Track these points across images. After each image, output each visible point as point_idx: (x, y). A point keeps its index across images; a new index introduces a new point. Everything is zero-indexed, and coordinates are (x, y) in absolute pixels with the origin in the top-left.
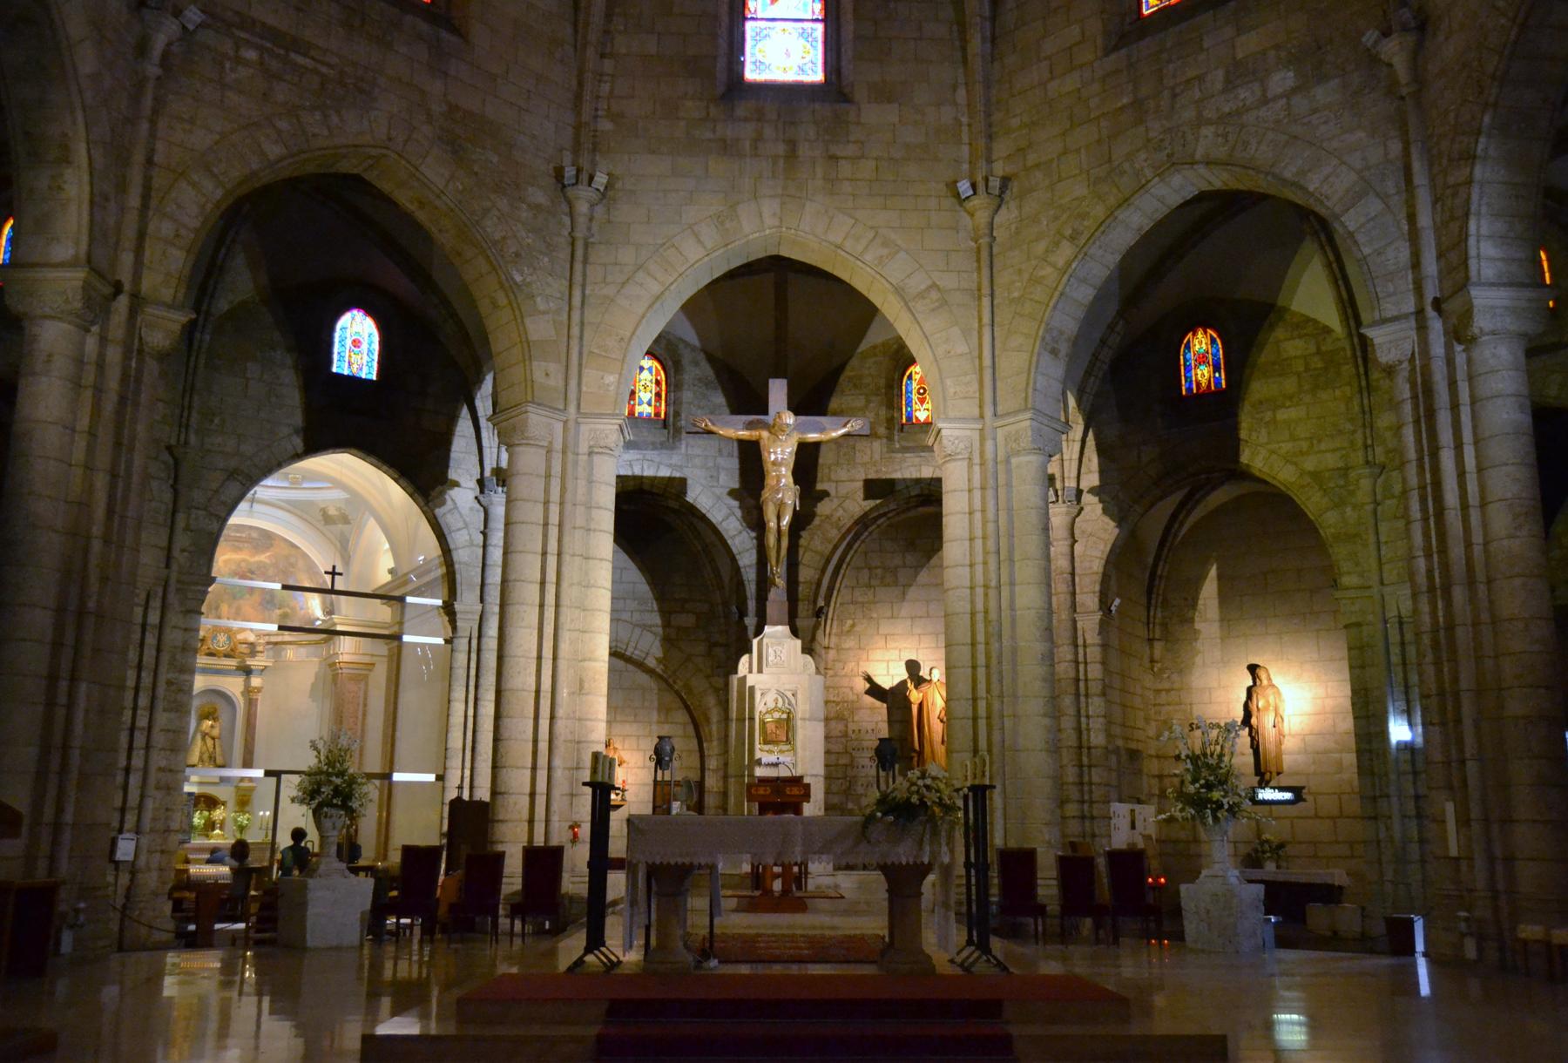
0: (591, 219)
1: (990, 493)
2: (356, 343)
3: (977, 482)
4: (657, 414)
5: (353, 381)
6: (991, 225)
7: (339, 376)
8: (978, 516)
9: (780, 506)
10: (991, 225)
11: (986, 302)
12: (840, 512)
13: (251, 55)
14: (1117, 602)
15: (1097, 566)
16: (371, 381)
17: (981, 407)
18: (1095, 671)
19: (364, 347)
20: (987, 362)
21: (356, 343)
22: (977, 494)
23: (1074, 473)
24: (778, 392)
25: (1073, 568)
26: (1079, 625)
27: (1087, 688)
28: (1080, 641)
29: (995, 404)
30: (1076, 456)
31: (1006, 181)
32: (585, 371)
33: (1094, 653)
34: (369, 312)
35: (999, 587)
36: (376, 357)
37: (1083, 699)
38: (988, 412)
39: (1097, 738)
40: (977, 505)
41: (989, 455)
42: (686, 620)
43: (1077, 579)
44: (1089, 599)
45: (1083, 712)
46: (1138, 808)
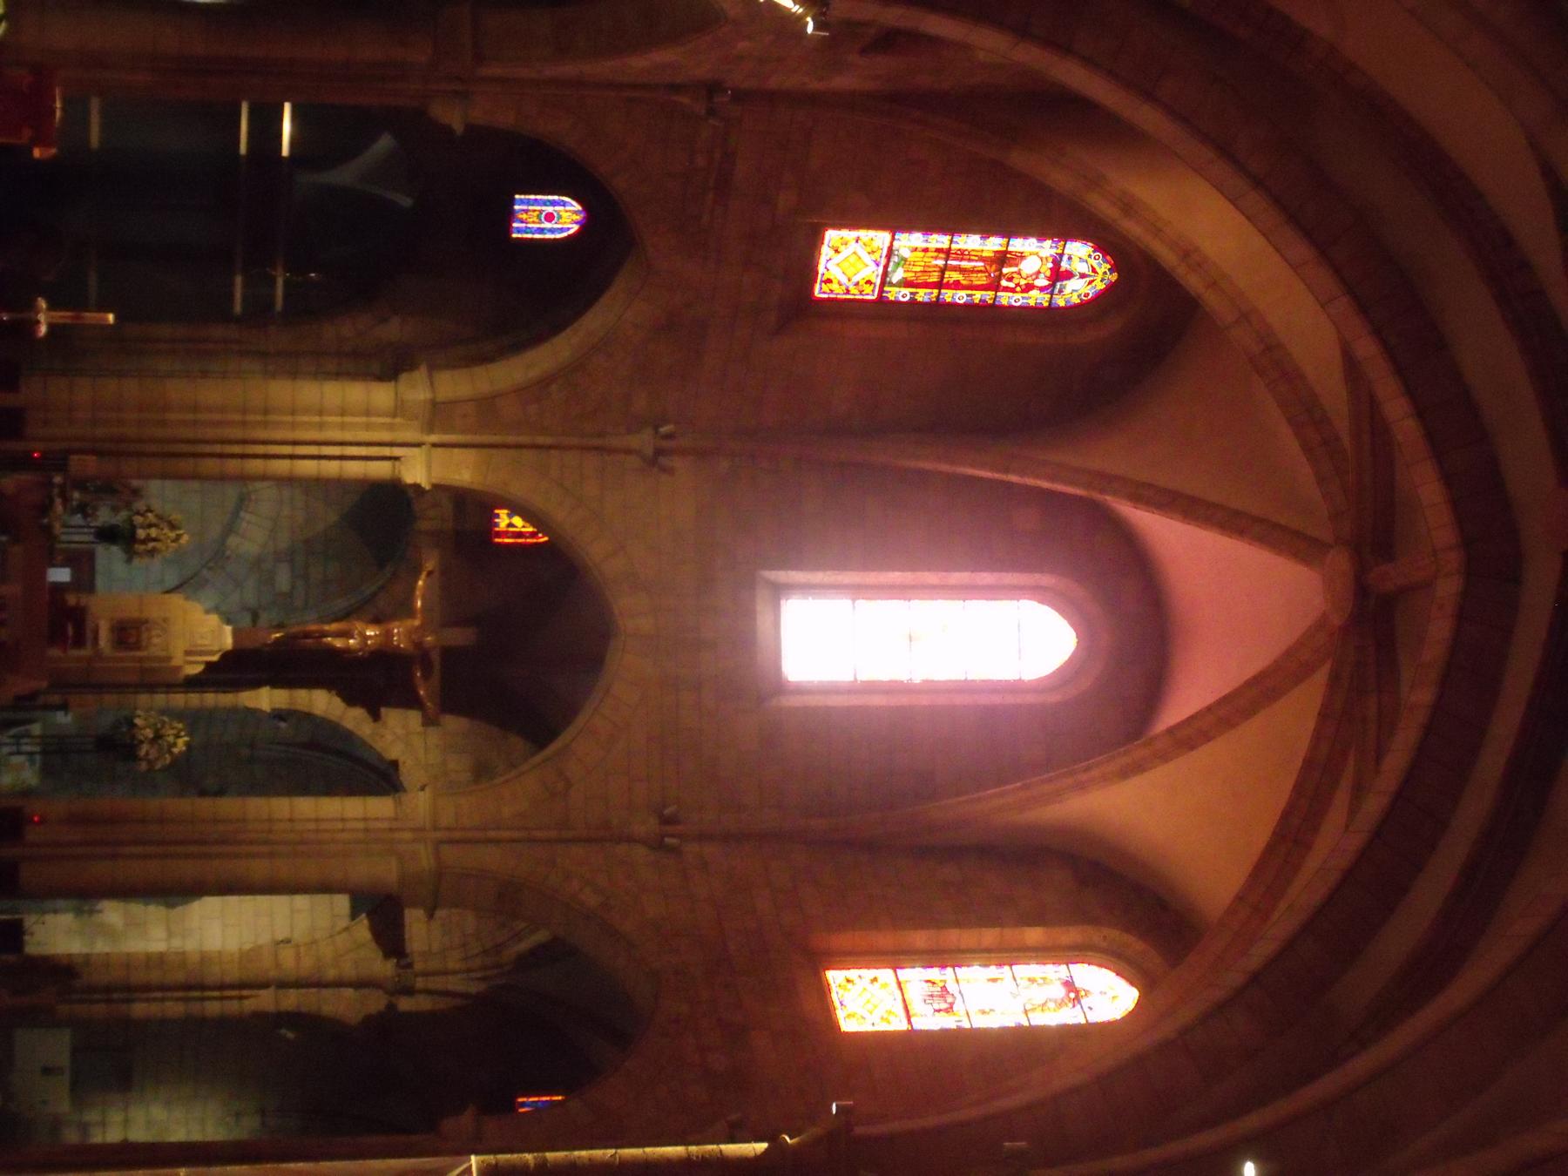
0: (628, 452)
1: (361, 836)
2: (550, 217)
3: (372, 825)
4: (499, 534)
5: (510, 215)
6: (630, 840)
7: (513, 202)
8: (340, 826)
9: (347, 634)
10: (630, 840)
11: (553, 834)
12: (389, 737)
13: (701, 161)
14: (290, 1035)
15: (328, 1009)
16: (509, 230)
17: (448, 829)
18: (213, 1008)
19: (547, 225)
20: (492, 834)
21: (550, 217)
22: (361, 825)
23: (431, 986)
24: (459, 637)
25: (327, 985)
26: (263, 992)
27: (194, 999)
28: (245, 993)
29: (451, 842)
30: (450, 987)
31: (675, 851)
32: (473, 452)
33: (233, 1007)
34: (585, 226)
35: (266, 842)
36: (537, 236)
37: (180, 994)
38: (439, 835)
39: (139, 1009)
40: (349, 825)
41: (397, 835)
42: (283, 580)
43: (314, 990)
44: (291, 1000)
45: (169, 994)
46: (66, 1078)
